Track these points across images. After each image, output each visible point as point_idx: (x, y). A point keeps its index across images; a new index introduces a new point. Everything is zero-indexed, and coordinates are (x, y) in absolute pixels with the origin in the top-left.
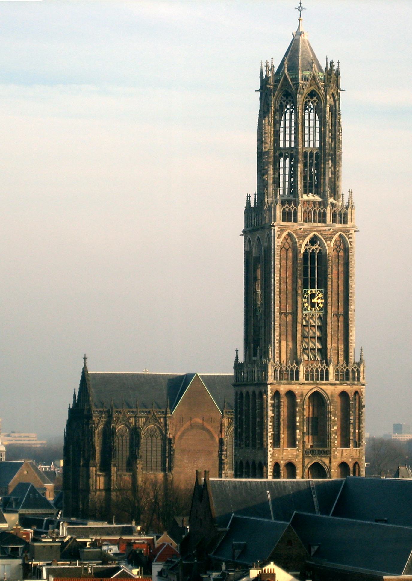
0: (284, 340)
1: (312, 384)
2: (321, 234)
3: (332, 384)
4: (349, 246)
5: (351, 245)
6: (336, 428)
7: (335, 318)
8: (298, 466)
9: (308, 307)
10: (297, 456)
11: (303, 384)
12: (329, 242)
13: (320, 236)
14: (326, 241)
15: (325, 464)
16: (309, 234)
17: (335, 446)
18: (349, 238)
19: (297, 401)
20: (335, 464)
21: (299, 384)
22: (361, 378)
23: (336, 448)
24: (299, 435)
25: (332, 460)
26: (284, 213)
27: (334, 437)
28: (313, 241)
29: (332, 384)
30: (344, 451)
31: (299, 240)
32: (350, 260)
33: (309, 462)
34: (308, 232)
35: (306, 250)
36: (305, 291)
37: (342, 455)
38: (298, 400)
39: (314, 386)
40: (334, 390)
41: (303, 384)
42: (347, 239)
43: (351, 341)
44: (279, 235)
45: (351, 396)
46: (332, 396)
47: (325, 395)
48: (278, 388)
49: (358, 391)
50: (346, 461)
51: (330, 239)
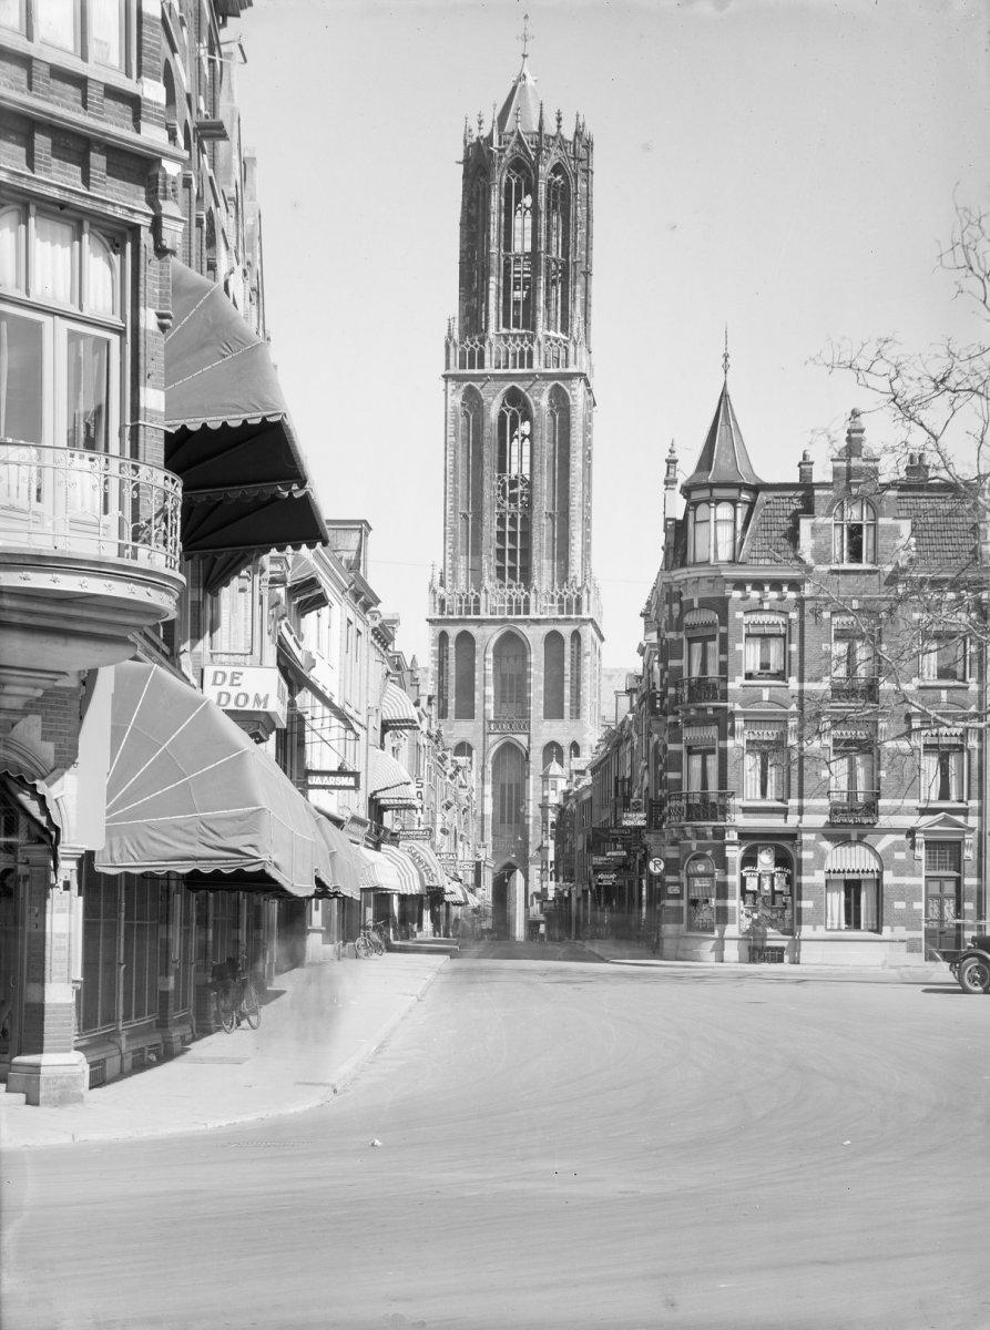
4: (571, 403)
18: (571, 390)
22: (584, 610)
26: (462, 354)
28: (514, 397)
29: (537, 622)
36: (499, 478)
47: (523, 638)
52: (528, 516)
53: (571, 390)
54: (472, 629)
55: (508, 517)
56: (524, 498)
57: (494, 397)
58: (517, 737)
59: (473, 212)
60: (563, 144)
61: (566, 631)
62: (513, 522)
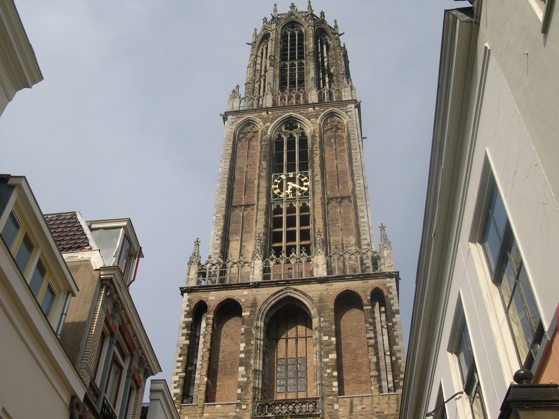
2: (301, 114)
3: (321, 281)
5: (350, 117)
9: (280, 193)
11: (257, 285)
12: (312, 119)
13: (300, 116)
14: (309, 119)
17: (331, 394)
19: (243, 314)
21: (247, 286)
23: (335, 395)
24: (243, 376)
27: (330, 375)
30: (356, 401)
32: (351, 133)
35: (280, 136)
37: (351, 412)
38: (245, 314)
40: (327, 290)
41: (257, 285)
42: (344, 113)
43: (362, 225)
44: (233, 122)
45: (366, 298)
46: (321, 300)
52: (309, 204)
53: (347, 113)
55: (284, 206)
59: (259, 61)
61: (362, 288)
62: (291, 210)
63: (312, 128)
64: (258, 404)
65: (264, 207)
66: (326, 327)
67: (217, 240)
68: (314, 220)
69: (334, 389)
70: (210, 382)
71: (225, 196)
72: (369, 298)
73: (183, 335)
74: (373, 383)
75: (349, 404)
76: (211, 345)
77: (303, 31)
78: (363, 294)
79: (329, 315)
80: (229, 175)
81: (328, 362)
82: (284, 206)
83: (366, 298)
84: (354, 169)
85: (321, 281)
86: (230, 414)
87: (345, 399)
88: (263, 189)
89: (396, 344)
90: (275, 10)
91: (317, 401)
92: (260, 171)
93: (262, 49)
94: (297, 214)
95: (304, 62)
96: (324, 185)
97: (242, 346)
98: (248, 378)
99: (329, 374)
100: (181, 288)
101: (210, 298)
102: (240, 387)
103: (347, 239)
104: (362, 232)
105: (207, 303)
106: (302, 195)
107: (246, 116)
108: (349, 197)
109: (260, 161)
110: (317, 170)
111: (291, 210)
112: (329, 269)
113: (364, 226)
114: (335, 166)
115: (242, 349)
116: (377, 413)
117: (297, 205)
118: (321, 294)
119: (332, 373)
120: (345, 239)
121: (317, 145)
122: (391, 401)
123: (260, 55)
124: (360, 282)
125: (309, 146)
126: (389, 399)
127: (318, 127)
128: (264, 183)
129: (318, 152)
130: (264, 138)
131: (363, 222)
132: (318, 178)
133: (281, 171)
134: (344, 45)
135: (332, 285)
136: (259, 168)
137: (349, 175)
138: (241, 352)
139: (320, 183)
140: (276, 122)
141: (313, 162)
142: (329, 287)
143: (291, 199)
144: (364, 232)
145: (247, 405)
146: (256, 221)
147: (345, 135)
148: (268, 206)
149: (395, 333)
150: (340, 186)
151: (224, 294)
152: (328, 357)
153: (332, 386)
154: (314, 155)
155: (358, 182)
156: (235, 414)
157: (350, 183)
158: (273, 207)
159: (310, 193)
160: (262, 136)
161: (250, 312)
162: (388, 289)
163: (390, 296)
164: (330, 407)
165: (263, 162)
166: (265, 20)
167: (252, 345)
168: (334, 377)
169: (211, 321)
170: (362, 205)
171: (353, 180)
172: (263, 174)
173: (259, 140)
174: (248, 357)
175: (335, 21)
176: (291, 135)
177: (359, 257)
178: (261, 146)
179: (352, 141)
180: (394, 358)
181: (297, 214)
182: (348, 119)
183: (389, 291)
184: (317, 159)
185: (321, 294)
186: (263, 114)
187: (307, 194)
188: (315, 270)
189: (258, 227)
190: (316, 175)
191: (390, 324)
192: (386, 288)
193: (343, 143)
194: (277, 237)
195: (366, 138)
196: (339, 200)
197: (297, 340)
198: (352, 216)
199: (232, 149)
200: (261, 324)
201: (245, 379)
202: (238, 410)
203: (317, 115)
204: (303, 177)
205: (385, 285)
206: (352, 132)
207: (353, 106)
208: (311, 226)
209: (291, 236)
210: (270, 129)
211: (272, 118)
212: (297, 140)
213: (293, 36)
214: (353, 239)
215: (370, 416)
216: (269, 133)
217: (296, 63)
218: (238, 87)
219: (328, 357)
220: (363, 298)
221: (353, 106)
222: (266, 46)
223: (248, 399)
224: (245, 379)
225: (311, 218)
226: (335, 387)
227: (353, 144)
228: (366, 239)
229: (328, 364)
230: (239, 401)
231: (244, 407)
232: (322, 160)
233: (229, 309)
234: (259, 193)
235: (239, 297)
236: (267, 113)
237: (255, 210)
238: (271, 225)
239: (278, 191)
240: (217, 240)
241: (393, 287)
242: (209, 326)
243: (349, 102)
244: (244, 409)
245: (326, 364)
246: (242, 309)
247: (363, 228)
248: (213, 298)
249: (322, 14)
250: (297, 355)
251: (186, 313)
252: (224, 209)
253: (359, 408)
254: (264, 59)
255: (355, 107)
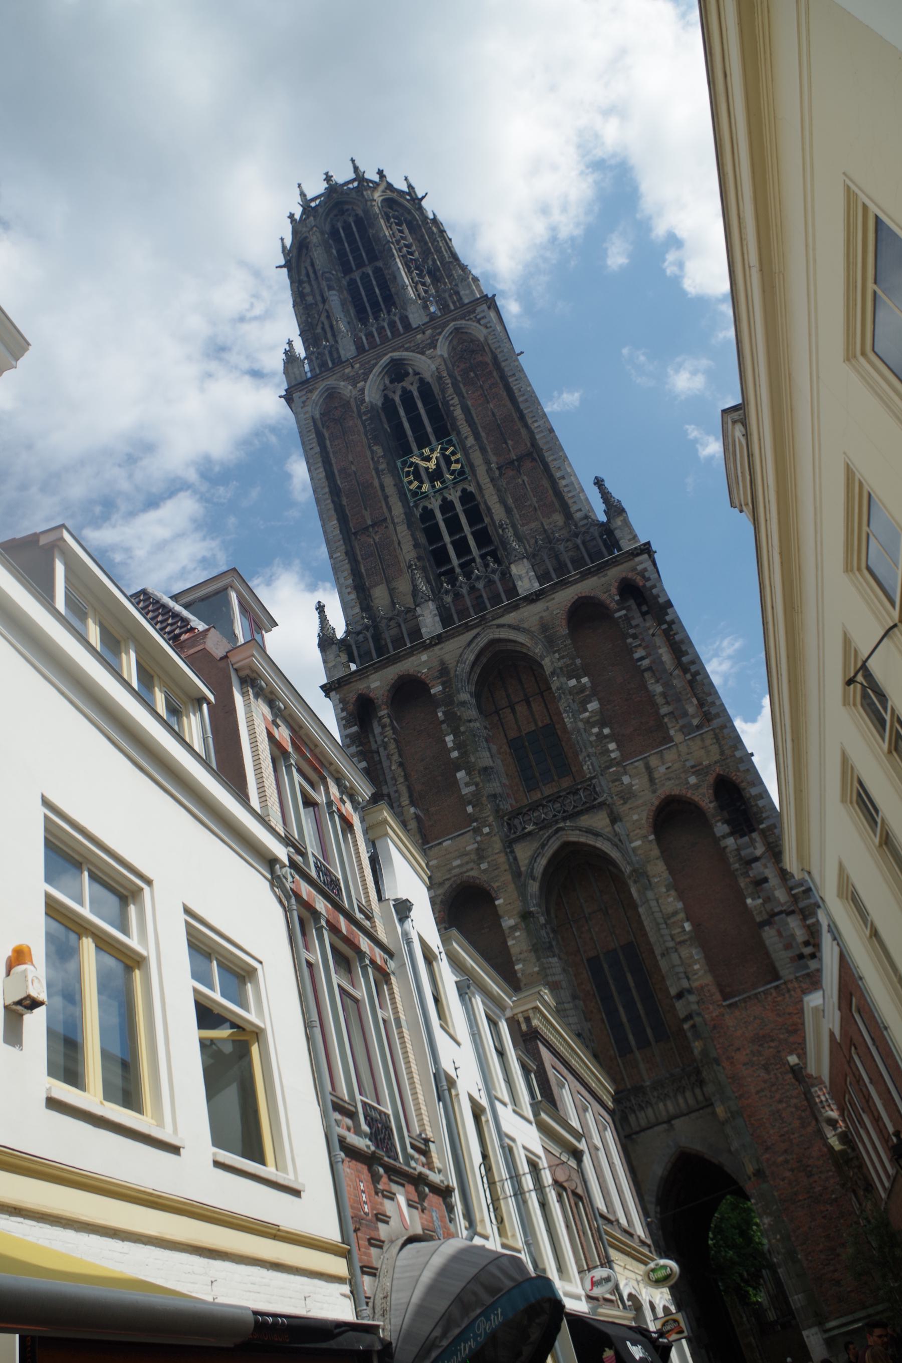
0: (376, 585)
1: (467, 628)
2: (407, 350)
3: (533, 598)
5: (487, 327)
6: (593, 706)
7: (511, 473)
8: (495, 885)
9: (420, 487)
10: (480, 854)
11: (439, 639)
12: (428, 352)
13: (405, 354)
14: (423, 353)
15: (597, 834)
16: (376, 364)
17: (612, 763)
19: (433, 691)
20: (638, 815)
23: (618, 764)
24: (467, 785)
25: (622, 809)
27: (600, 736)
30: (654, 762)
31: (354, 385)
32: (497, 352)
33: (533, 856)
34: (372, 362)
35: (386, 397)
36: (404, 463)
37: (652, 780)
38: (436, 690)
39: (474, 632)
40: (548, 609)
41: (439, 639)
42: (475, 324)
43: (566, 490)
44: (304, 402)
45: (611, 598)
46: (544, 627)
47: (521, 638)
48: (361, 686)
49: (630, 575)
50: (676, 792)
51: (433, 345)
52: (471, 488)
53: (478, 321)
54: (408, 666)
55: (435, 505)
56: (455, 467)
57: (365, 380)
58: (586, 821)
59: (307, 290)
60: (390, 186)
61: (600, 586)
62: (447, 506)
63: (433, 367)
64: (506, 818)
65: (403, 516)
66: (567, 666)
67: (349, 593)
68: (489, 509)
69: (613, 755)
70: (419, 813)
71: (335, 522)
72: (617, 598)
73: (353, 756)
74: (670, 725)
75: (644, 770)
76: (400, 756)
77: (360, 213)
78: (606, 595)
79: (565, 646)
80: (329, 487)
81: (589, 718)
82: (435, 505)
83: (611, 598)
84: (522, 406)
85: (533, 598)
86: (468, 848)
87: (636, 764)
88: (391, 490)
89: (686, 653)
90: (303, 195)
91: (594, 781)
92: (376, 463)
93: (306, 268)
94: (459, 508)
95: (380, 264)
96: (483, 450)
97: (449, 739)
98: (477, 785)
99: (597, 735)
100: (322, 687)
101: (373, 686)
102: (470, 803)
103: (551, 520)
104: (570, 502)
105: (372, 695)
106: (455, 478)
107: (322, 386)
108: (532, 453)
109: (370, 447)
110: (465, 430)
111: (447, 506)
112: (542, 577)
113: (569, 492)
114: (490, 413)
115: (450, 745)
116: (692, 767)
117: (454, 496)
118: (541, 618)
119: (601, 732)
120: (546, 522)
121: (451, 391)
122: (708, 742)
123: (305, 279)
124: (595, 578)
125: (439, 397)
126: (703, 740)
127: (439, 360)
128: (388, 481)
129: (456, 401)
130: (363, 409)
131: (566, 486)
132: (471, 441)
133: (408, 452)
134: (434, 215)
135: (553, 599)
136: (373, 459)
137: (517, 419)
138: (454, 749)
139: (477, 448)
140: (371, 376)
141: (454, 419)
142: (549, 604)
143: (441, 489)
144: (573, 500)
145: (489, 826)
146: (399, 543)
147: (488, 359)
148: (409, 514)
149: (677, 638)
150: (510, 443)
151: (391, 673)
152: (586, 710)
153: (608, 751)
154: (452, 408)
155: (536, 425)
156: (476, 845)
157: (523, 431)
158: (418, 513)
159: (467, 470)
160: (358, 407)
161: (442, 685)
162: (642, 574)
163: (648, 584)
164: (617, 783)
165: (375, 448)
166: (291, 216)
167: (464, 732)
168: (606, 737)
169: (386, 720)
170: (555, 460)
171: (526, 426)
172: (383, 466)
173: (355, 415)
174: (464, 754)
175: (406, 179)
176: (404, 390)
177: (579, 541)
178: (363, 423)
179: (503, 364)
180: (689, 676)
181: (459, 508)
182: (485, 331)
183: (643, 577)
184: (458, 413)
185: (541, 618)
186: (347, 371)
187: (462, 472)
188: (519, 584)
189: (405, 551)
190: (466, 438)
191: (665, 626)
192: (638, 574)
193: (490, 373)
194: (440, 557)
195: (522, 353)
196: (516, 464)
197: (528, 703)
198: (545, 483)
199: (319, 445)
200: (464, 696)
201: (473, 788)
202: (479, 839)
203: (432, 342)
204: (447, 449)
205: (634, 569)
206: (499, 350)
207: (485, 307)
208: (487, 520)
209: (462, 547)
210: (366, 392)
211: (363, 373)
212: (416, 394)
213: (347, 227)
214: (558, 518)
215: (683, 776)
216: (367, 399)
217: (369, 270)
218: (290, 343)
219: (586, 710)
220: (608, 602)
221: (485, 307)
222: (309, 260)
223: (488, 816)
224: (473, 788)
225: (482, 507)
226: (613, 751)
227: (506, 369)
228: (580, 510)
229: (591, 720)
230: (475, 824)
231: (486, 830)
232: (466, 410)
233: (409, 691)
234: (386, 498)
235: (416, 669)
236: (353, 367)
237: (391, 526)
238: (422, 540)
239: (416, 484)
240: (349, 593)
241: (649, 569)
242: (387, 729)
243: (476, 302)
244: (488, 834)
245: (587, 721)
246: (427, 685)
247: (570, 495)
248: (377, 684)
249: (380, 173)
250: (536, 725)
251: (344, 722)
252: (341, 542)
253: (662, 769)
254: (313, 282)
255: (489, 308)
